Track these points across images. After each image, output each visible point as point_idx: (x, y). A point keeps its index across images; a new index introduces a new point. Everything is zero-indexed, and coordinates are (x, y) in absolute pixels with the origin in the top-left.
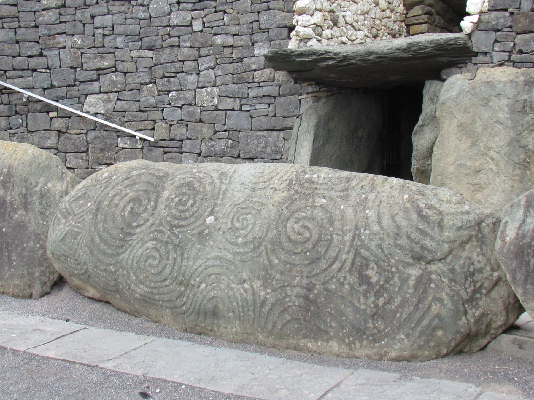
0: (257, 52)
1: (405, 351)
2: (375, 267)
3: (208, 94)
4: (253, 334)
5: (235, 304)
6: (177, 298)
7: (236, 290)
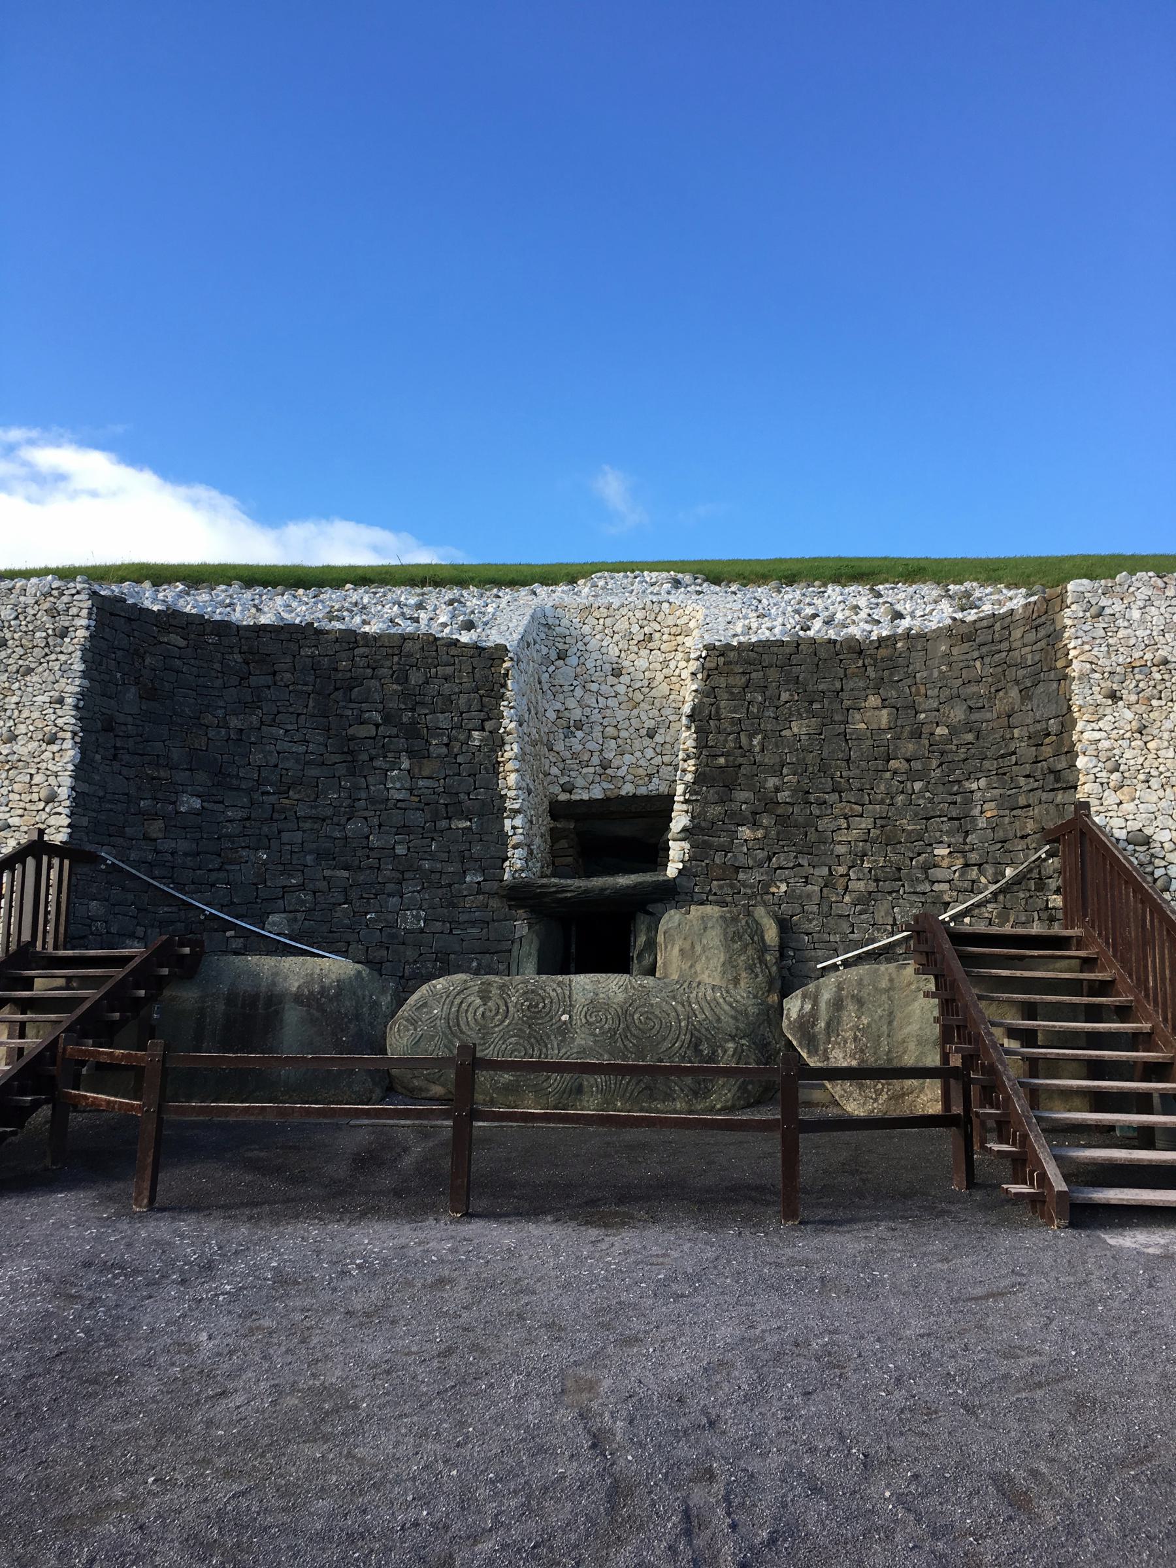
0: (468, 879)
3: (413, 916)
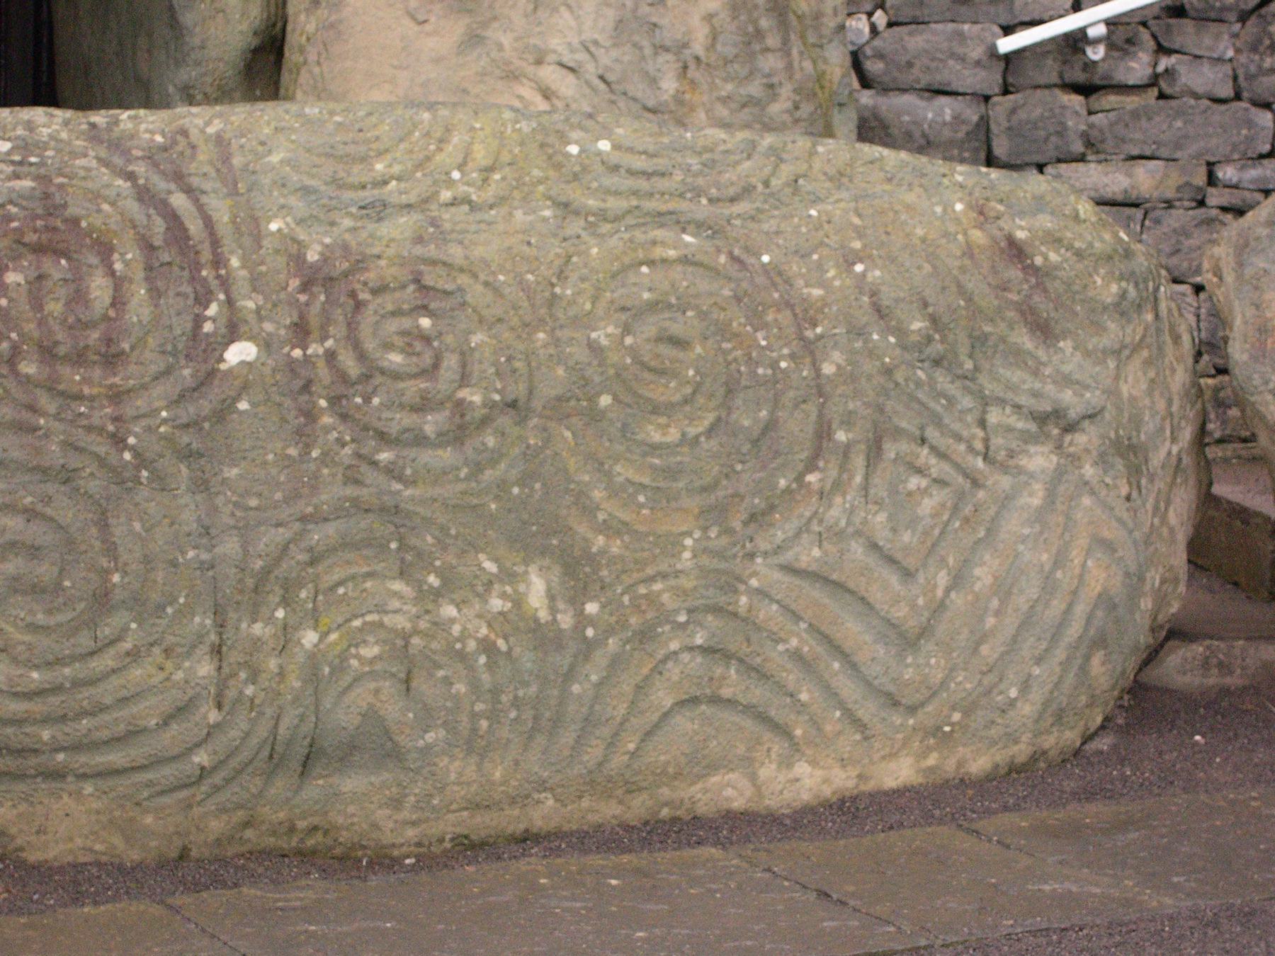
1: (1016, 742)
2: (933, 461)
4: (513, 801)
5: (460, 688)
6: (166, 722)
7: (456, 630)
